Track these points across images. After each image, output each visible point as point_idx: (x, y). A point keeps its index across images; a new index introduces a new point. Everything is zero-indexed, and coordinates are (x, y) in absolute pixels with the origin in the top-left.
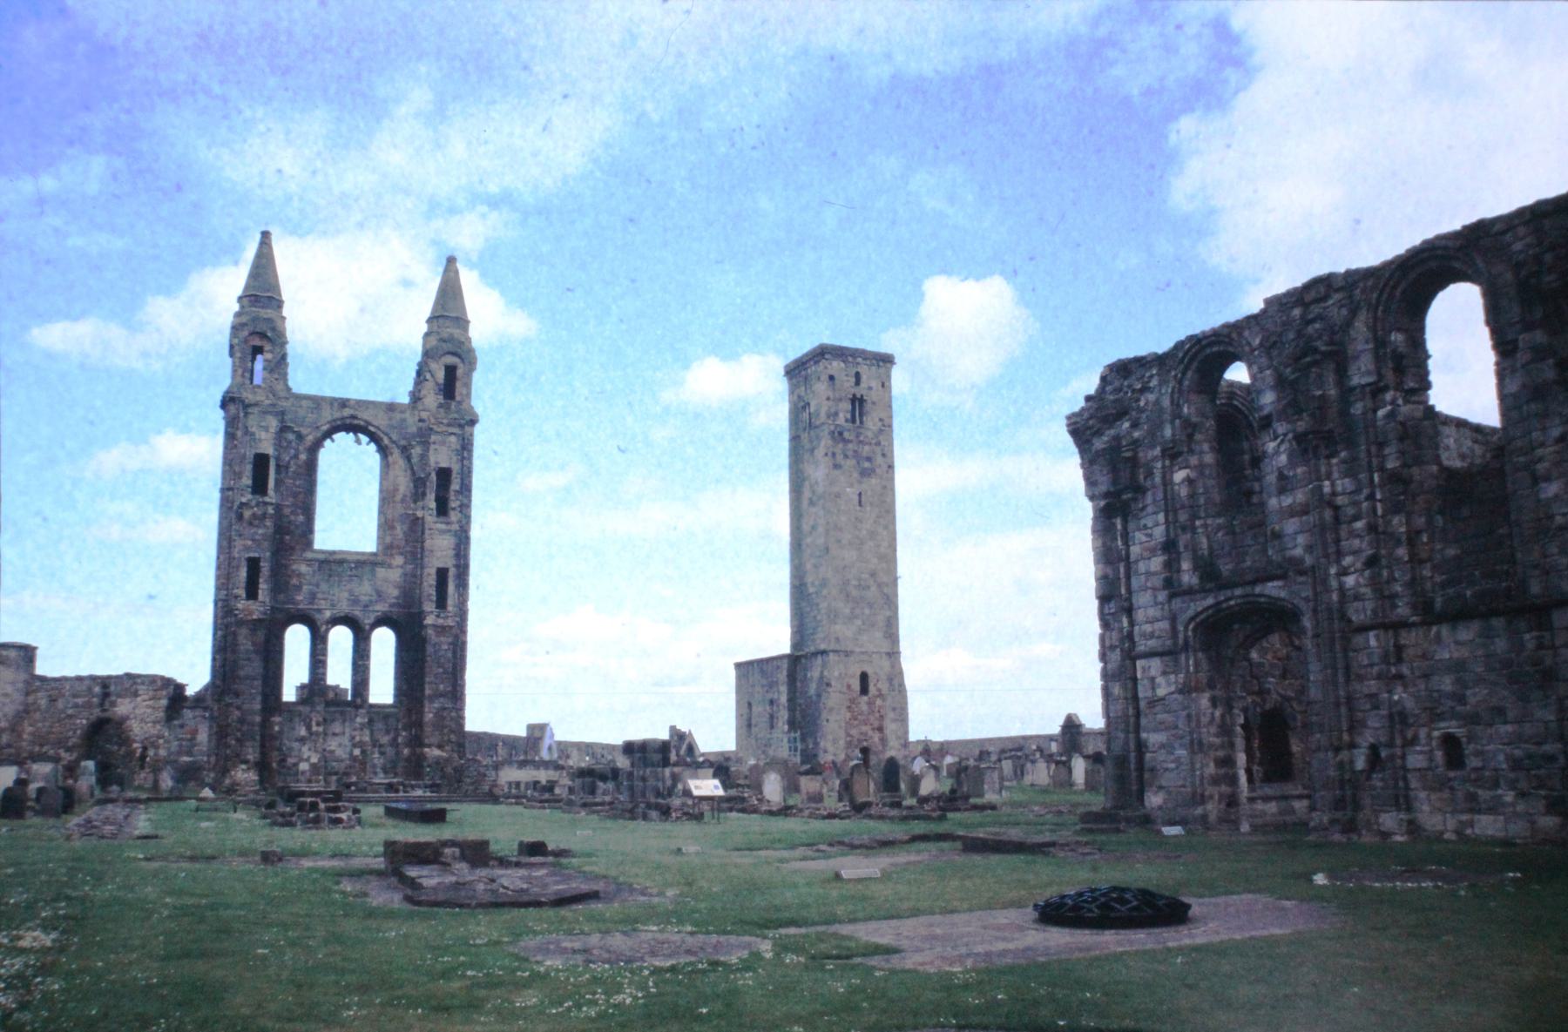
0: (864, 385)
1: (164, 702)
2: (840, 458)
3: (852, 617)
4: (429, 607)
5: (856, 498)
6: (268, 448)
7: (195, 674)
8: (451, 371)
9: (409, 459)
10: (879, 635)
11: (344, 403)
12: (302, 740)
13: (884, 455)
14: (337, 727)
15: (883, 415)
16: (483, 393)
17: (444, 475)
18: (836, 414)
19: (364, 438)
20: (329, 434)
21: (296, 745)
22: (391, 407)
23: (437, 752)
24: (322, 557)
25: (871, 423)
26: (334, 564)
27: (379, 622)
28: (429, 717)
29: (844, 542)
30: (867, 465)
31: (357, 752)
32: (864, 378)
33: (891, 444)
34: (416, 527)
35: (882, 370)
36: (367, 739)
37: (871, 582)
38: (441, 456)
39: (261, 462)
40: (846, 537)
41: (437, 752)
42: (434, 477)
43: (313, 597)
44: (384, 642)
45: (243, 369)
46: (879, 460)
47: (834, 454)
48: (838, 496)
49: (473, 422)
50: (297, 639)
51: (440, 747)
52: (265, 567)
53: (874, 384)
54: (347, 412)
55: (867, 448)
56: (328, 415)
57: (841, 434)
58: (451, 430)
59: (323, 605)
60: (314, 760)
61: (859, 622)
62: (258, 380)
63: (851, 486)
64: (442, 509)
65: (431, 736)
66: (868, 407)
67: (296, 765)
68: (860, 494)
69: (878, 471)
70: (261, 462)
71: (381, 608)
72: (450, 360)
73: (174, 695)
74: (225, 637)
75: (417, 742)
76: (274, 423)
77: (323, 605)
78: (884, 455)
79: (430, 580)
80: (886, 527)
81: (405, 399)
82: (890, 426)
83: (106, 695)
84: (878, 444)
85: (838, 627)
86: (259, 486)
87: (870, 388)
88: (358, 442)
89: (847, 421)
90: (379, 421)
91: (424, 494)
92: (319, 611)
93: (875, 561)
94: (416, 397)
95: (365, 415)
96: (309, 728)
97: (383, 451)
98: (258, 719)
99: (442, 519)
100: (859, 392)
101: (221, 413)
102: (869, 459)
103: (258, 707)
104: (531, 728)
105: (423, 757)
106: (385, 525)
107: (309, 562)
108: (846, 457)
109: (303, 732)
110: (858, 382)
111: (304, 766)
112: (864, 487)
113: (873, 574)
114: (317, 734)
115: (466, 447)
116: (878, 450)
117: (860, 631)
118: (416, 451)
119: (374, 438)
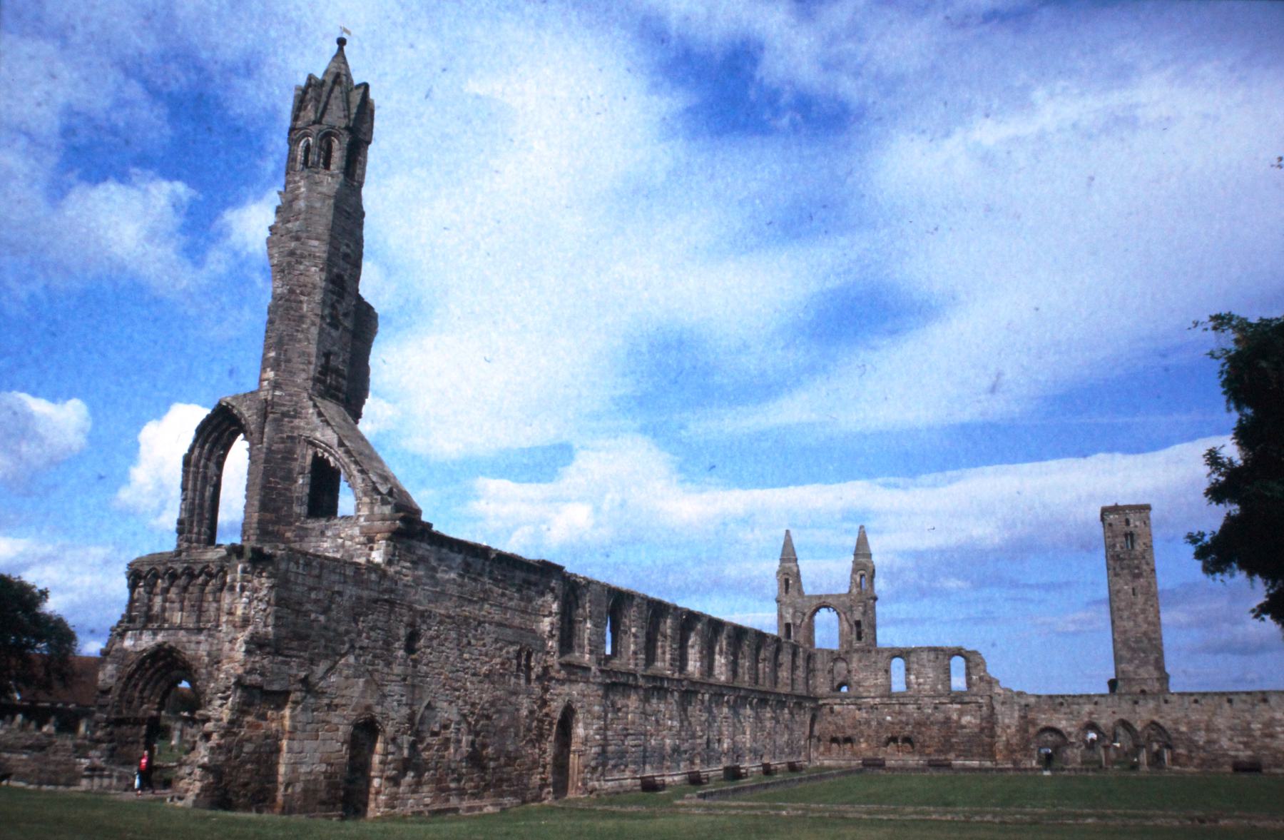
0: (1132, 525)
2: (1118, 570)
3: (1130, 661)
5: (1131, 591)
6: (790, 621)
10: (1151, 668)
11: (820, 597)
13: (1148, 564)
15: (1146, 541)
18: (1114, 546)
22: (839, 596)
25: (1139, 547)
29: (1125, 617)
30: (1136, 571)
32: (1132, 521)
33: (1152, 557)
35: (1143, 515)
37: (1144, 639)
39: (788, 626)
40: (1126, 614)
46: (1145, 567)
47: (1114, 569)
48: (1119, 591)
53: (1138, 523)
54: (822, 600)
55: (1136, 562)
56: (815, 602)
57: (1118, 556)
61: (1137, 662)
63: (1127, 584)
66: (1135, 537)
68: (1133, 589)
69: (1144, 574)
72: (862, 572)
76: (791, 611)
78: (1148, 564)
80: (1152, 606)
82: (1151, 546)
84: (1144, 558)
85: (1123, 666)
87: (1136, 526)
89: (1122, 548)
93: (1146, 626)
95: (830, 600)
97: (838, 614)
100: (1127, 529)
102: (1138, 567)
108: (1122, 569)
110: (1127, 522)
112: (1135, 584)
113: (1145, 634)
116: (1143, 562)
117: (1138, 667)
119: (834, 610)
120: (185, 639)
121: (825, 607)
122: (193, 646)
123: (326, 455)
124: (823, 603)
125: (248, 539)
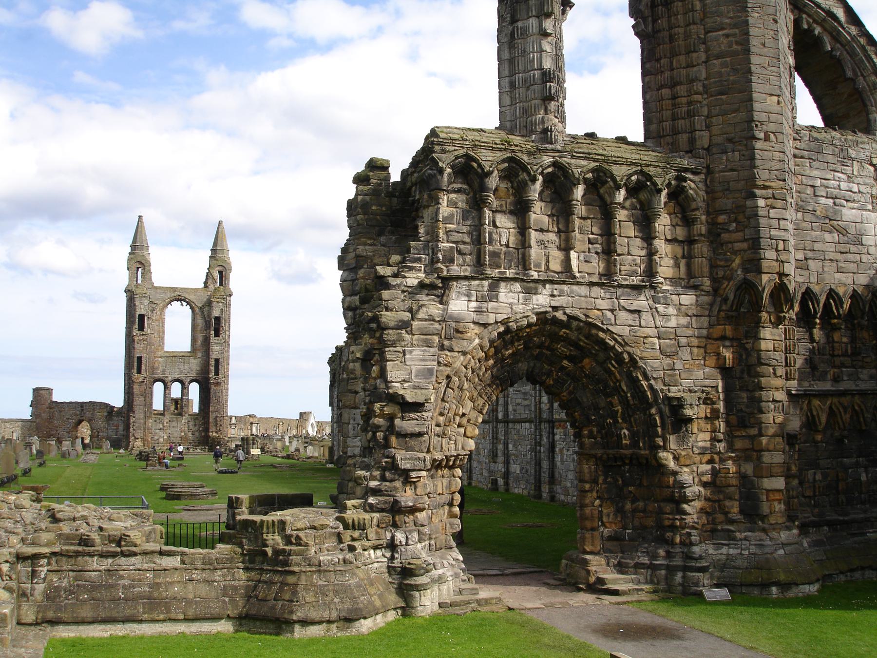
1: (105, 414)
4: (212, 374)
6: (143, 312)
7: (117, 400)
8: (221, 273)
9: (203, 312)
11: (174, 289)
12: (161, 429)
14: (174, 424)
16: (235, 282)
17: (218, 319)
19: (185, 304)
20: (170, 303)
21: (157, 431)
23: (215, 434)
24: (167, 354)
26: (174, 357)
27: (192, 381)
28: (211, 420)
31: (183, 434)
34: (206, 341)
36: (186, 429)
38: (216, 313)
41: (215, 434)
42: (213, 320)
43: (164, 372)
44: (194, 390)
45: (133, 277)
49: (230, 295)
50: (158, 387)
51: (216, 432)
52: (144, 362)
54: (177, 293)
56: (170, 295)
58: (220, 300)
59: (167, 374)
60: (165, 437)
62: (139, 282)
64: (217, 334)
65: (212, 428)
67: (158, 439)
70: (142, 317)
71: (194, 375)
72: (221, 269)
73: (109, 410)
74: (129, 388)
75: (207, 430)
76: (146, 301)
77: (167, 374)
79: (213, 362)
81: (202, 285)
83: (82, 410)
86: (141, 328)
88: (182, 305)
90: (191, 297)
91: (210, 328)
92: (166, 377)
94: (206, 283)
96: (163, 425)
97: (192, 308)
98: (142, 421)
99: (217, 338)
101: (125, 295)
103: (142, 416)
104: (301, 414)
105: (208, 436)
106: (194, 340)
107: (160, 356)
109: (161, 427)
111: (161, 440)
114: (167, 426)
115: (228, 305)
118: (206, 309)
119: (188, 303)
120: (603, 304)
121: (178, 300)
122: (623, 315)
123: (818, 30)
124: (179, 295)
125: (767, 139)
